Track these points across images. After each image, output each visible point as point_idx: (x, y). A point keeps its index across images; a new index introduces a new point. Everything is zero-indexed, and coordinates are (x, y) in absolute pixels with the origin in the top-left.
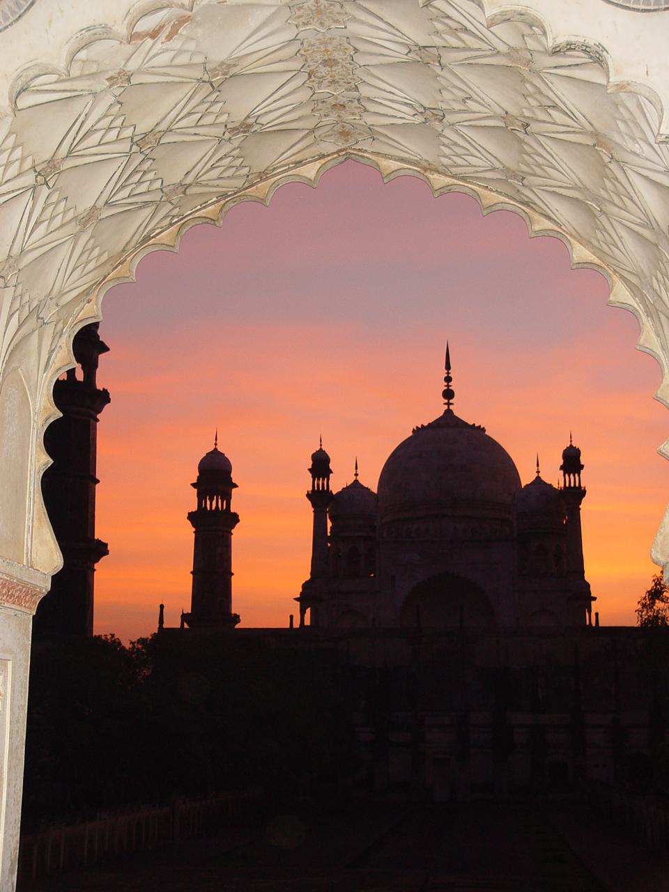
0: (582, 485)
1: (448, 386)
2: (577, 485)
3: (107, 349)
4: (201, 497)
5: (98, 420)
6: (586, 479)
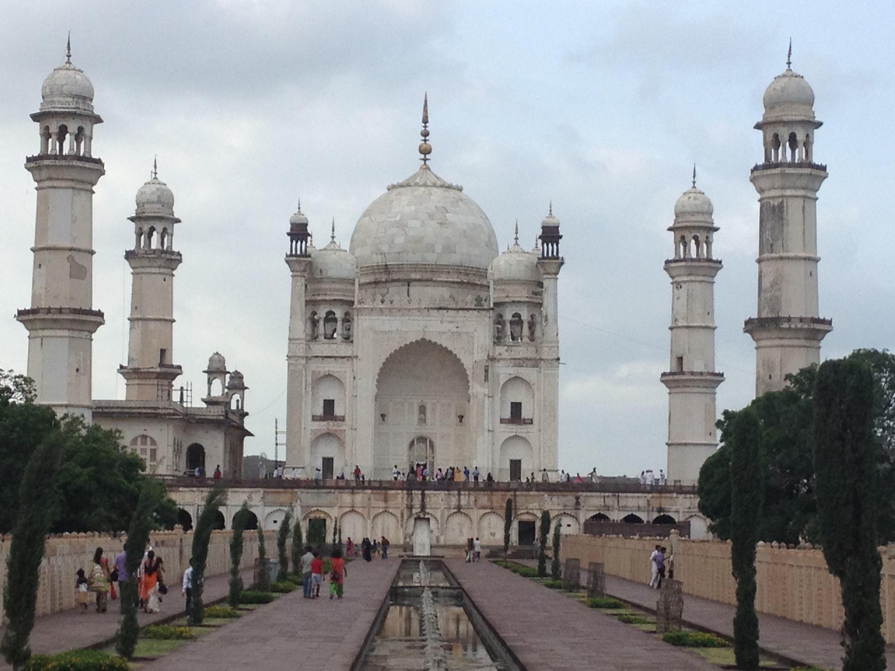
0: (560, 256)
1: (425, 141)
2: (555, 254)
3: (101, 121)
4: (139, 234)
5: (94, 192)
6: (564, 248)
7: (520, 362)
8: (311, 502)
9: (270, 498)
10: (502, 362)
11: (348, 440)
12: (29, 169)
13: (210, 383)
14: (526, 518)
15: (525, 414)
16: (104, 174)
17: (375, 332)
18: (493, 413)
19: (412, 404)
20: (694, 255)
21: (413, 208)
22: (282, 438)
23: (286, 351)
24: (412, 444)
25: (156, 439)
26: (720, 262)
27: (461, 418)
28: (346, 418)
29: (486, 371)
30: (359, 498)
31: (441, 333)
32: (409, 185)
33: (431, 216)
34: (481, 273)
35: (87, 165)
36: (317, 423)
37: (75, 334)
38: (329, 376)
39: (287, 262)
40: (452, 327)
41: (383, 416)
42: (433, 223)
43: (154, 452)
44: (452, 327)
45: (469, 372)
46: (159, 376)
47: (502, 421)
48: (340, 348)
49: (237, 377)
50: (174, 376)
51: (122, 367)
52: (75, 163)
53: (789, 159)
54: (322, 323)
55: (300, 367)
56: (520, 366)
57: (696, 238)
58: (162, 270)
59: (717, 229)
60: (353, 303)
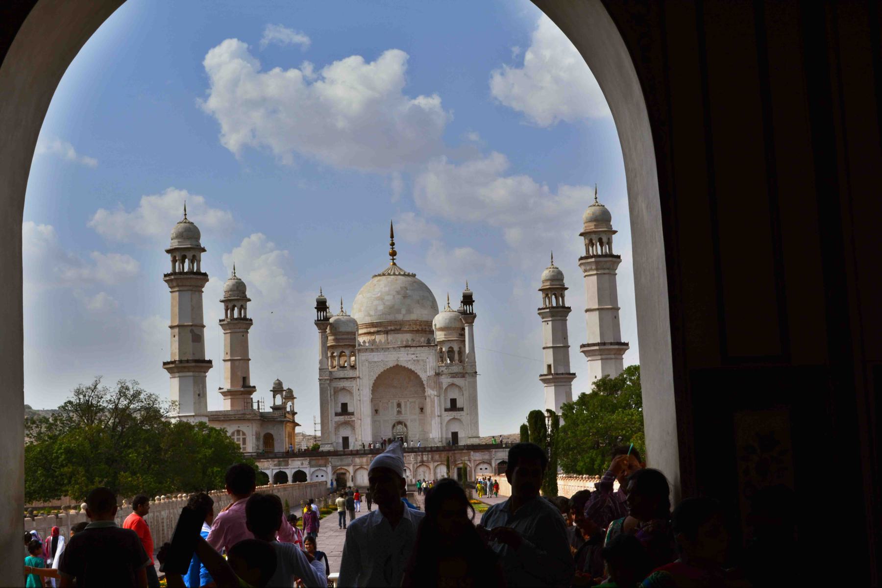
6: (476, 308)
7: (454, 375)
8: (338, 464)
9: (313, 462)
10: (443, 377)
11: (357, 425)
12: (166, 281)
13: (274, 397)
14: (461, 466)
15: (459, 405)
16: (208, 280)
17: (369, 363)
18: (440, 406)
20: (554, 305)
21: (387, 289)
22: (319, 427)
23: (318, 376)
24: (394, 426)
25: (245, 431)
26: (569, 308)
27: (422, 409)
30: (364, 460)
32: (384, 275)
33: (398, 293)
34: (429, 324)
35: (199, 277)
37: (197, 374)
38: (344, 389)
39: (316, 324)
41: (376, 411)
42: (400, 296)
43: (244, 440)
45: (425, 383)
46: (242, 393)
47: (446, 410)
49: (290, 391)
50: (251, 393)
51: (220, 389)
52: (192, 276)
53: (600, 253)
56: (454, 377)
57: (555, 294)
59: (567, 289)
60: (354, 346)
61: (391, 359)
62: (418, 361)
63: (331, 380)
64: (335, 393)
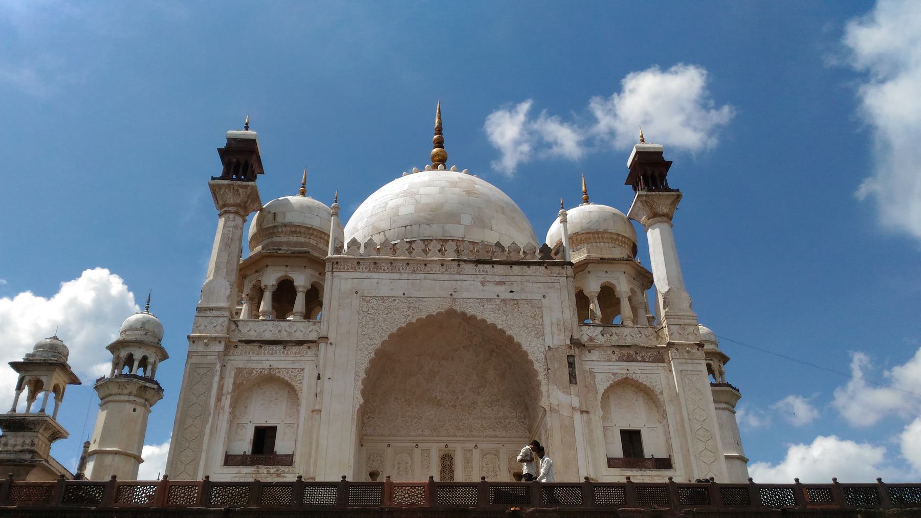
4: (116, 365)
7: (631, 353)
10: (595, 355)
17: (363, 297)
19: (426, 452)
28: (297, 459)
29: (571, 365)
31: (483, 301)
36: (234, 470)
38: (271, 379)
40: (503, 292)
44: (503, 292)
45: (537, 366)
48: (294, 326)
54: (268, 296)
55: (212, 358)
56: (630, 359)
58: (132, 398)
61: (432, 292)
62: (516, 302)
63: (230, 346)
64: (237, 386)
